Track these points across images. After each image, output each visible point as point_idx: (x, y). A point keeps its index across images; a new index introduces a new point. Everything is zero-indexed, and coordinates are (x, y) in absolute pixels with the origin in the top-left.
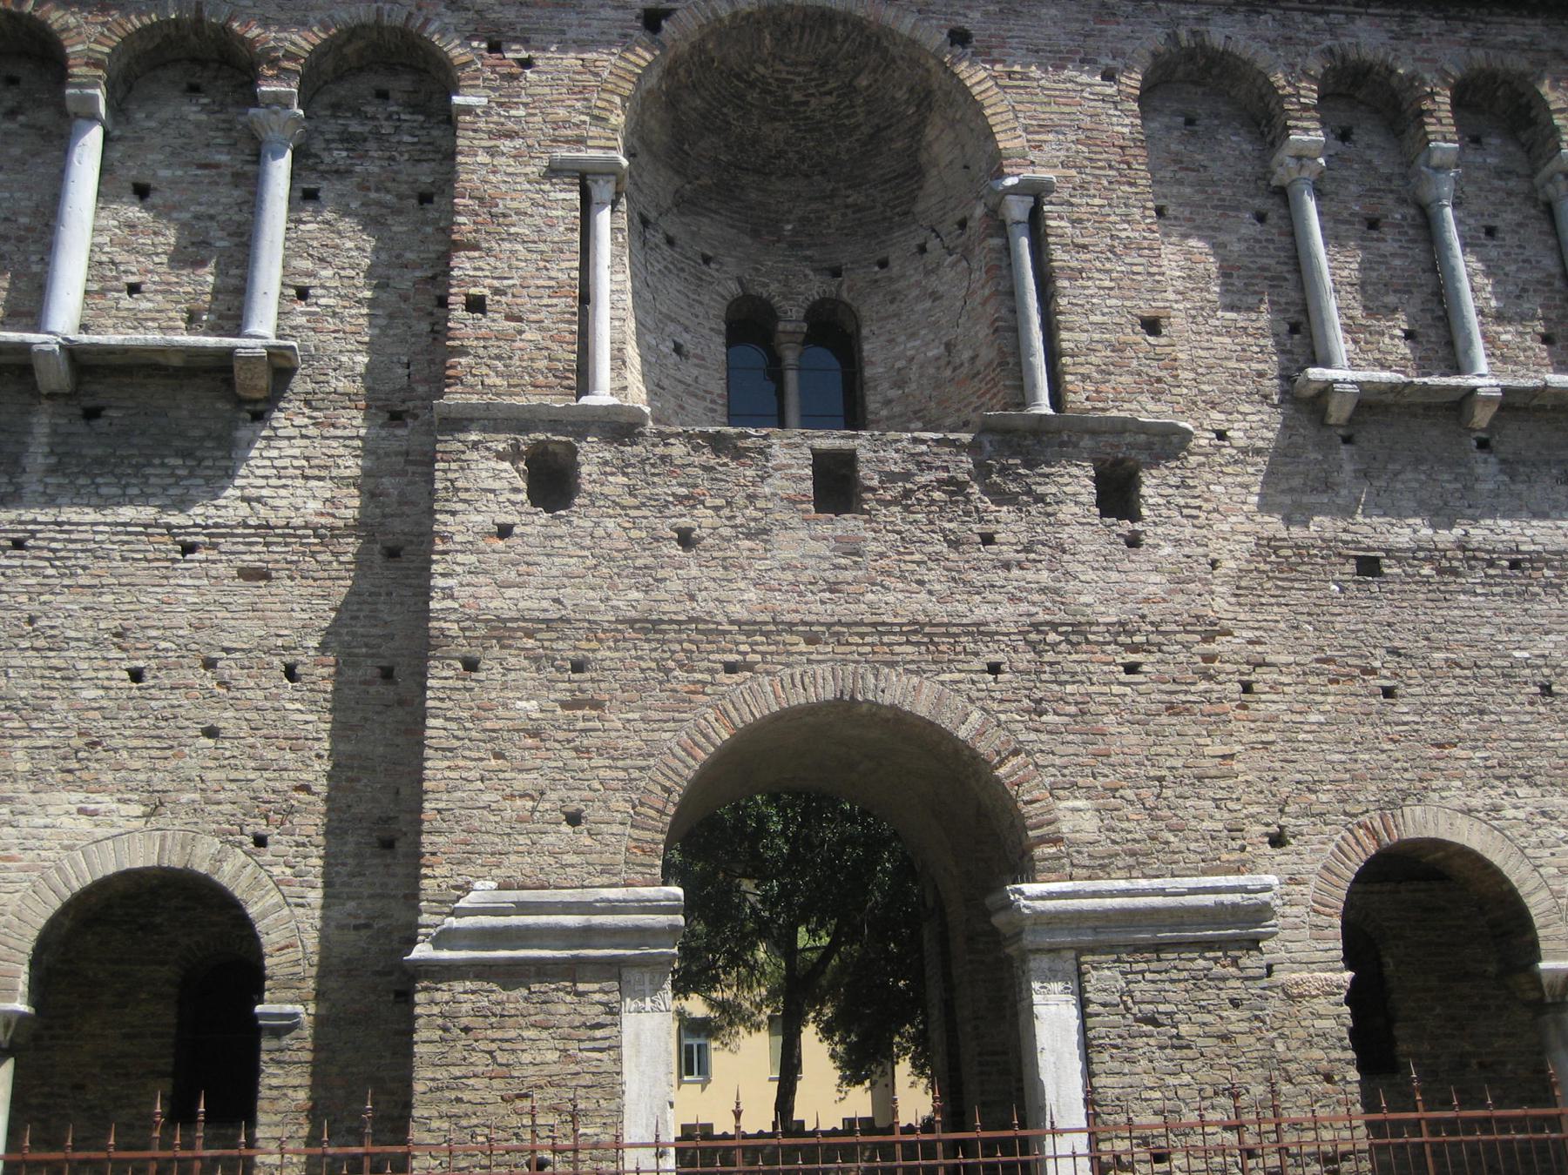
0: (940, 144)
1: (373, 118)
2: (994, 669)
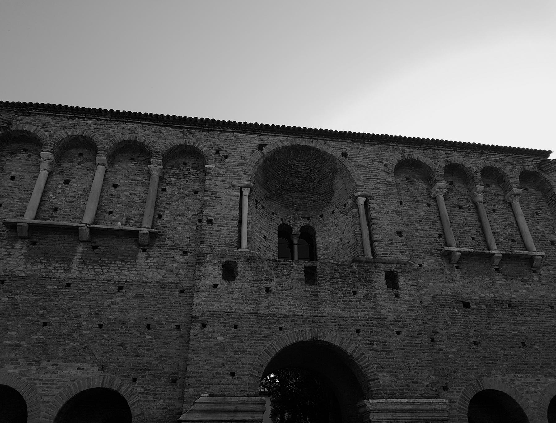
0: (339, 184)
1: (183, 170)
2: (358, 331)
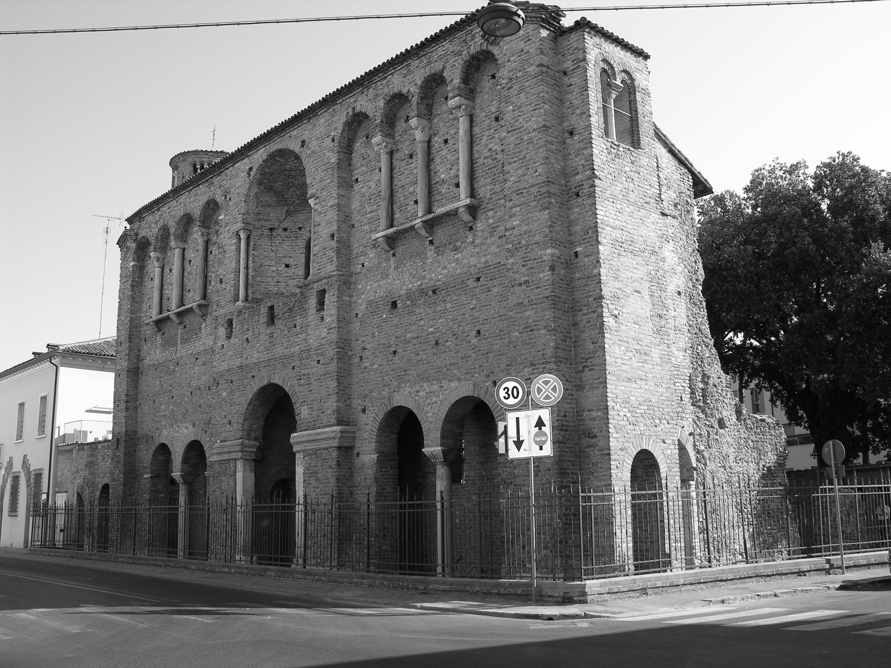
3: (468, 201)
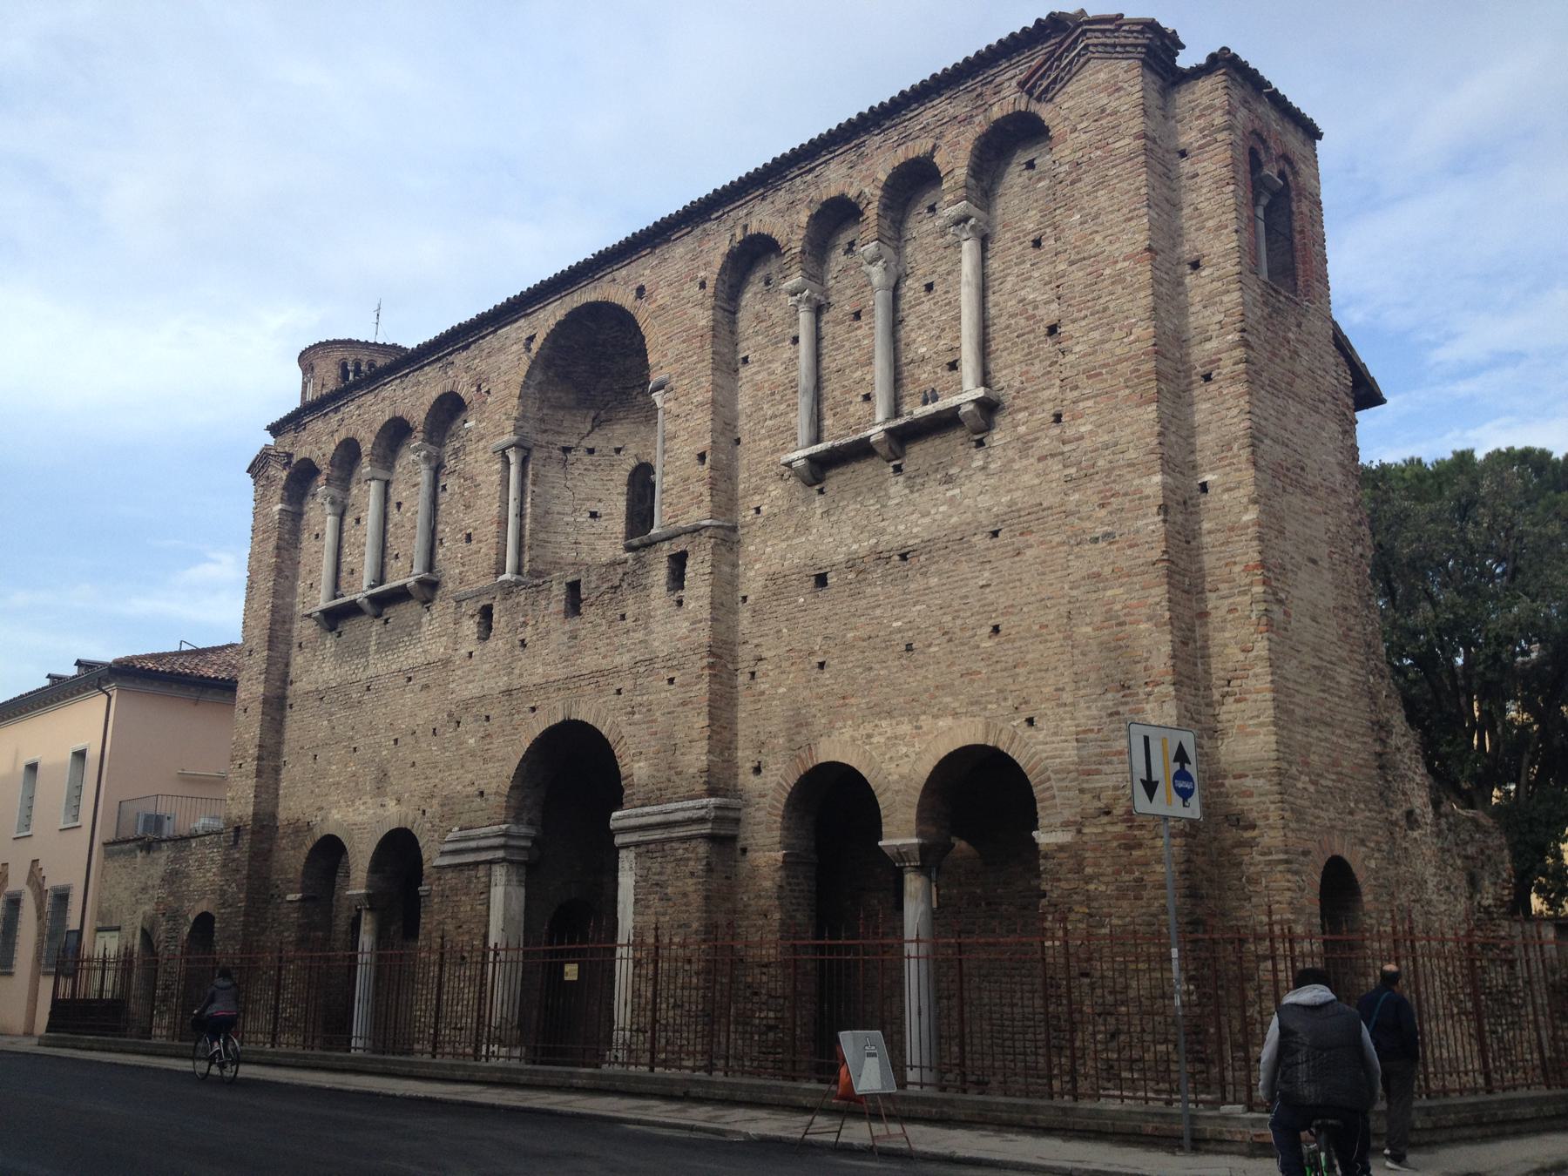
2: (619, 692)
3: (980, 392)
